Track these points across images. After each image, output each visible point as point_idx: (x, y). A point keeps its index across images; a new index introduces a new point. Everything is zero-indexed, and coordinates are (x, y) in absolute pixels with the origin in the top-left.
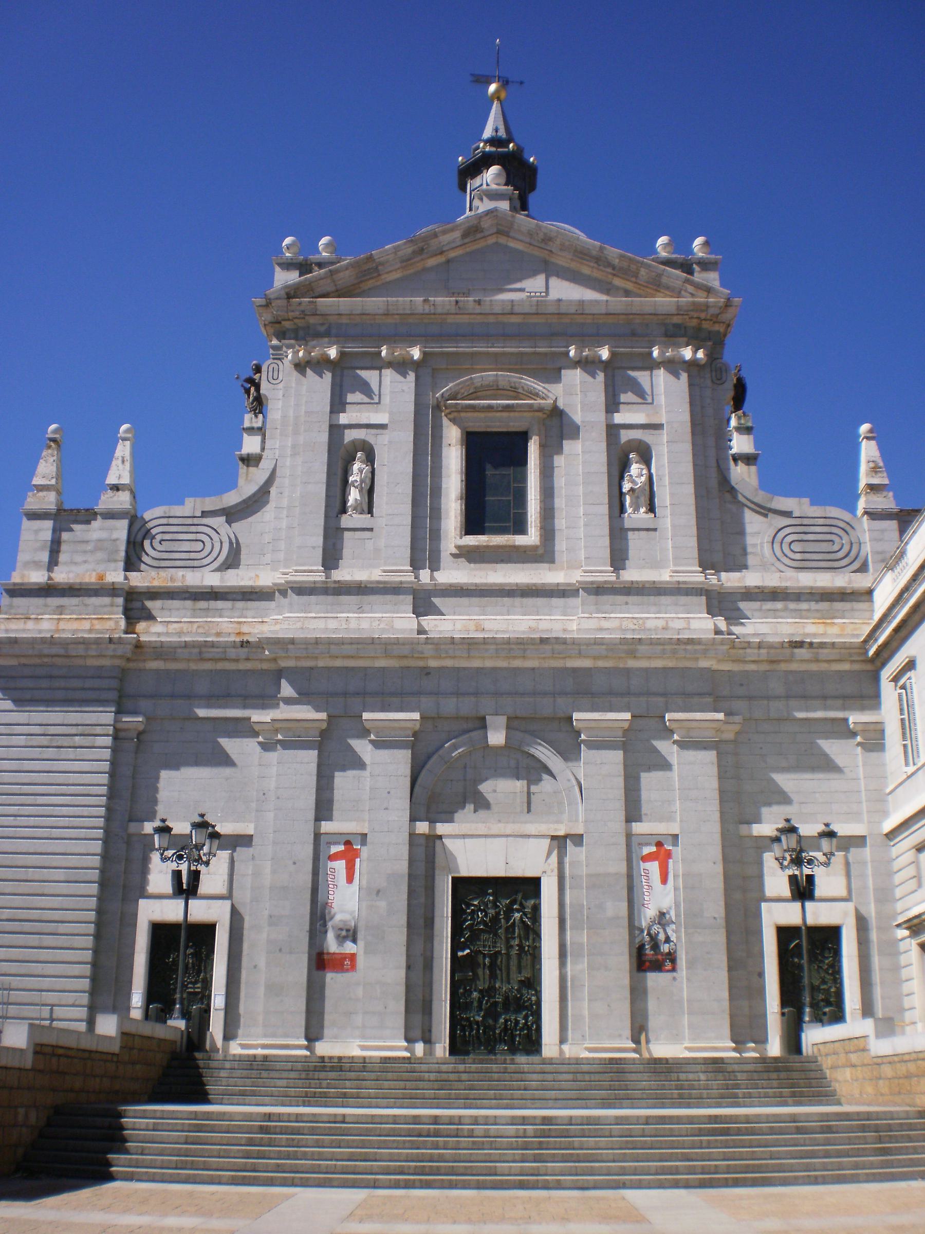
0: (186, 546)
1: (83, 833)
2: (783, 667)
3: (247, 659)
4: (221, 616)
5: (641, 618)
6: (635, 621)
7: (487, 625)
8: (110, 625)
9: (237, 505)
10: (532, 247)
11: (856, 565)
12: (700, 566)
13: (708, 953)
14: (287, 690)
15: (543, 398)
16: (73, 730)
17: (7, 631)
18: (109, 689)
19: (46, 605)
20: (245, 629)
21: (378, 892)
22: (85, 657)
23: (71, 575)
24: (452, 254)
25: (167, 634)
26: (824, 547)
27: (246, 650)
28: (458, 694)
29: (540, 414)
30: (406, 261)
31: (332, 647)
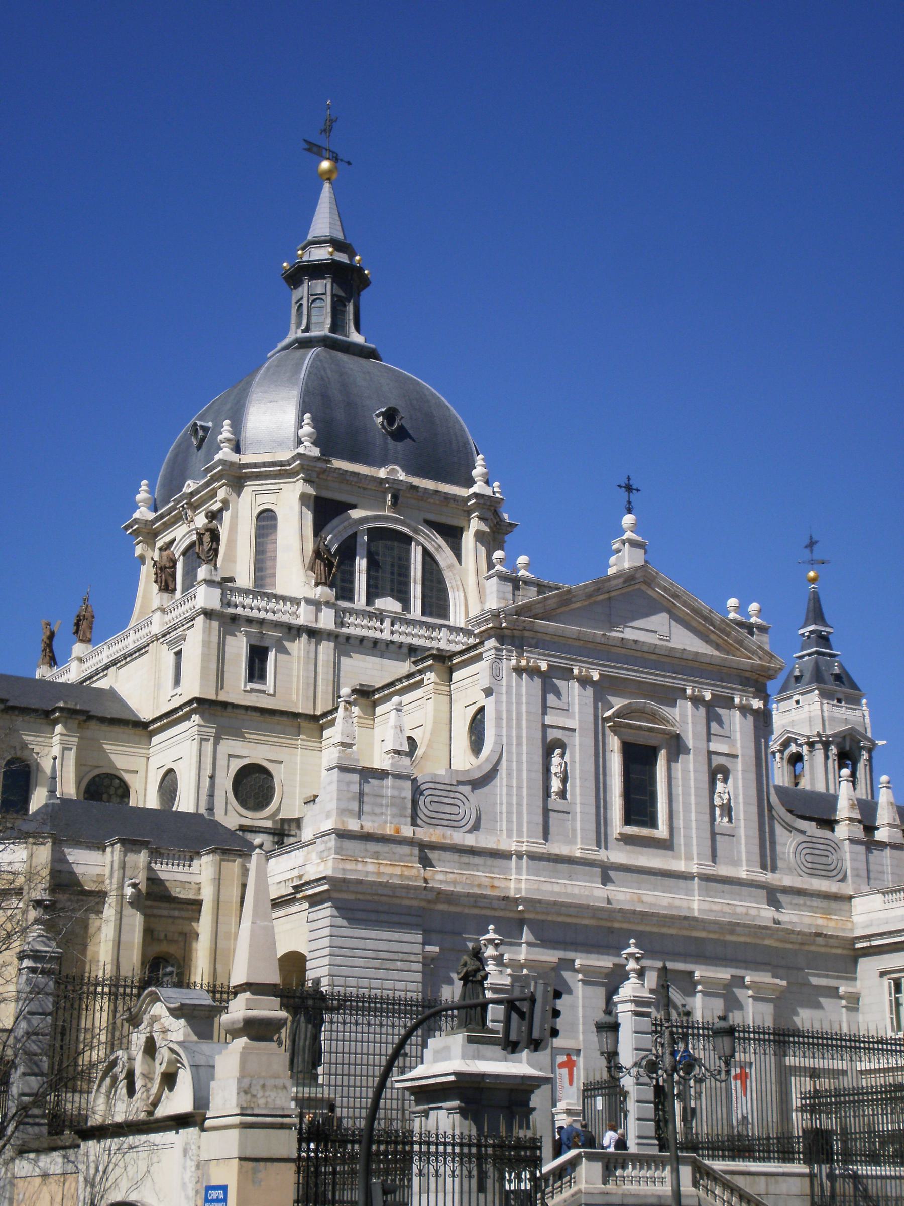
0: (448, 809)
2: (806, 948)
4: (478, 871)
7: (645, 899)
8: (414, 872)
11: (840, 877)
14: (527, 935)
15: (673, 726)
16: (395, 956)
19: (366, 850)
20: (496, 883)
22: (402, 898)
23: (376, 825)
24: (613, 594)
25: (446, 882)
26: (823, 860)
30: (589, 596)
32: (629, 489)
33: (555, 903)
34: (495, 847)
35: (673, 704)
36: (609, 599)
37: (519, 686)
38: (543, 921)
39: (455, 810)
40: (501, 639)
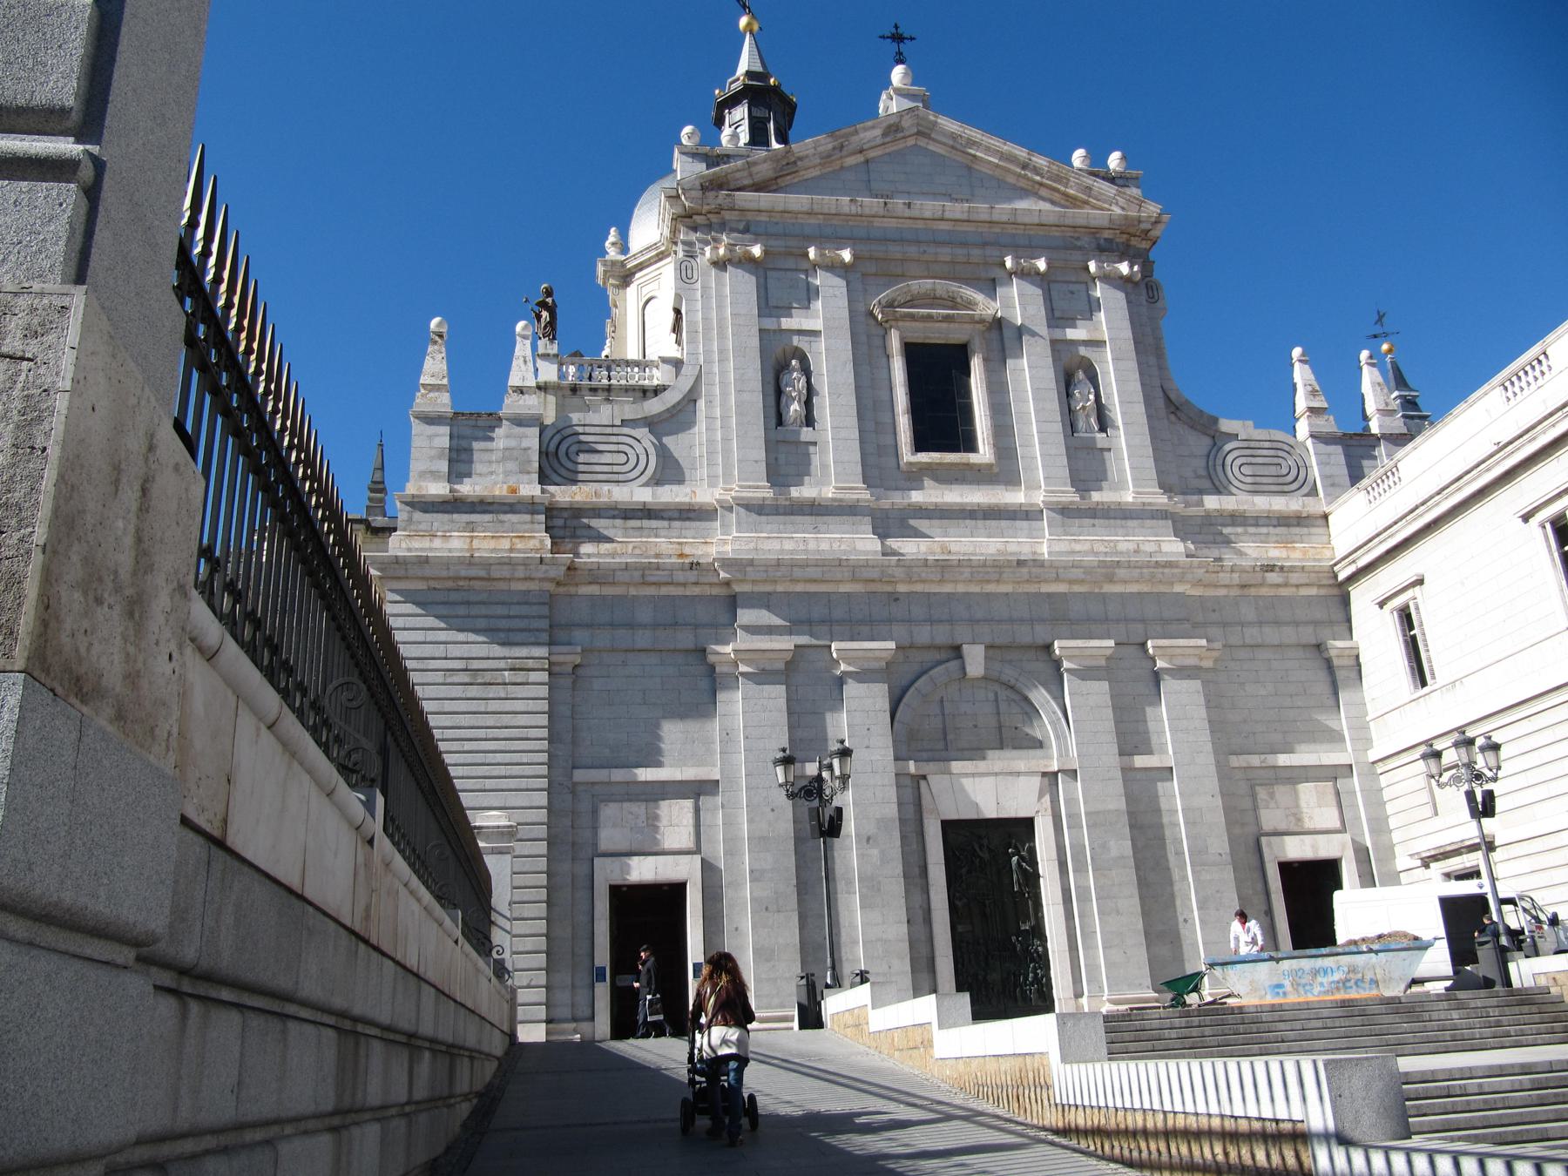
1: (523, 783)
3: (696, 584)
4: (656, 536)
5: (1111, 541)
6: (1106, 544)
7: (954, 548)
8: (532, 544)
9: (660, 414)
10: (954, 152)
11: (1305, 490)
12: (1160, 488)
13: (1218, 891)
17: (409, 550)
18: (540, 617)
19: (453, 521)
20: (687, 550)
21: (868, 839)
24: (872, 154)
26: (1273, 470)
27: (695, 572)
28: (931, 621)
29: (979, 326)
30: (827, 158)
31: (795, 569)
32: (898, 38)
33: (779, 563)
34: (687, 500)
35: (990, 286)
36: (867, 161)
37: (719, 283)
38: (769, 593)
39: (623, 458)
40: (695, 229)
